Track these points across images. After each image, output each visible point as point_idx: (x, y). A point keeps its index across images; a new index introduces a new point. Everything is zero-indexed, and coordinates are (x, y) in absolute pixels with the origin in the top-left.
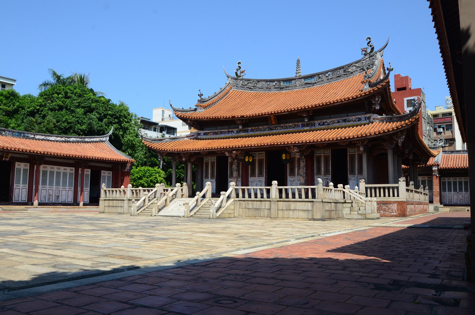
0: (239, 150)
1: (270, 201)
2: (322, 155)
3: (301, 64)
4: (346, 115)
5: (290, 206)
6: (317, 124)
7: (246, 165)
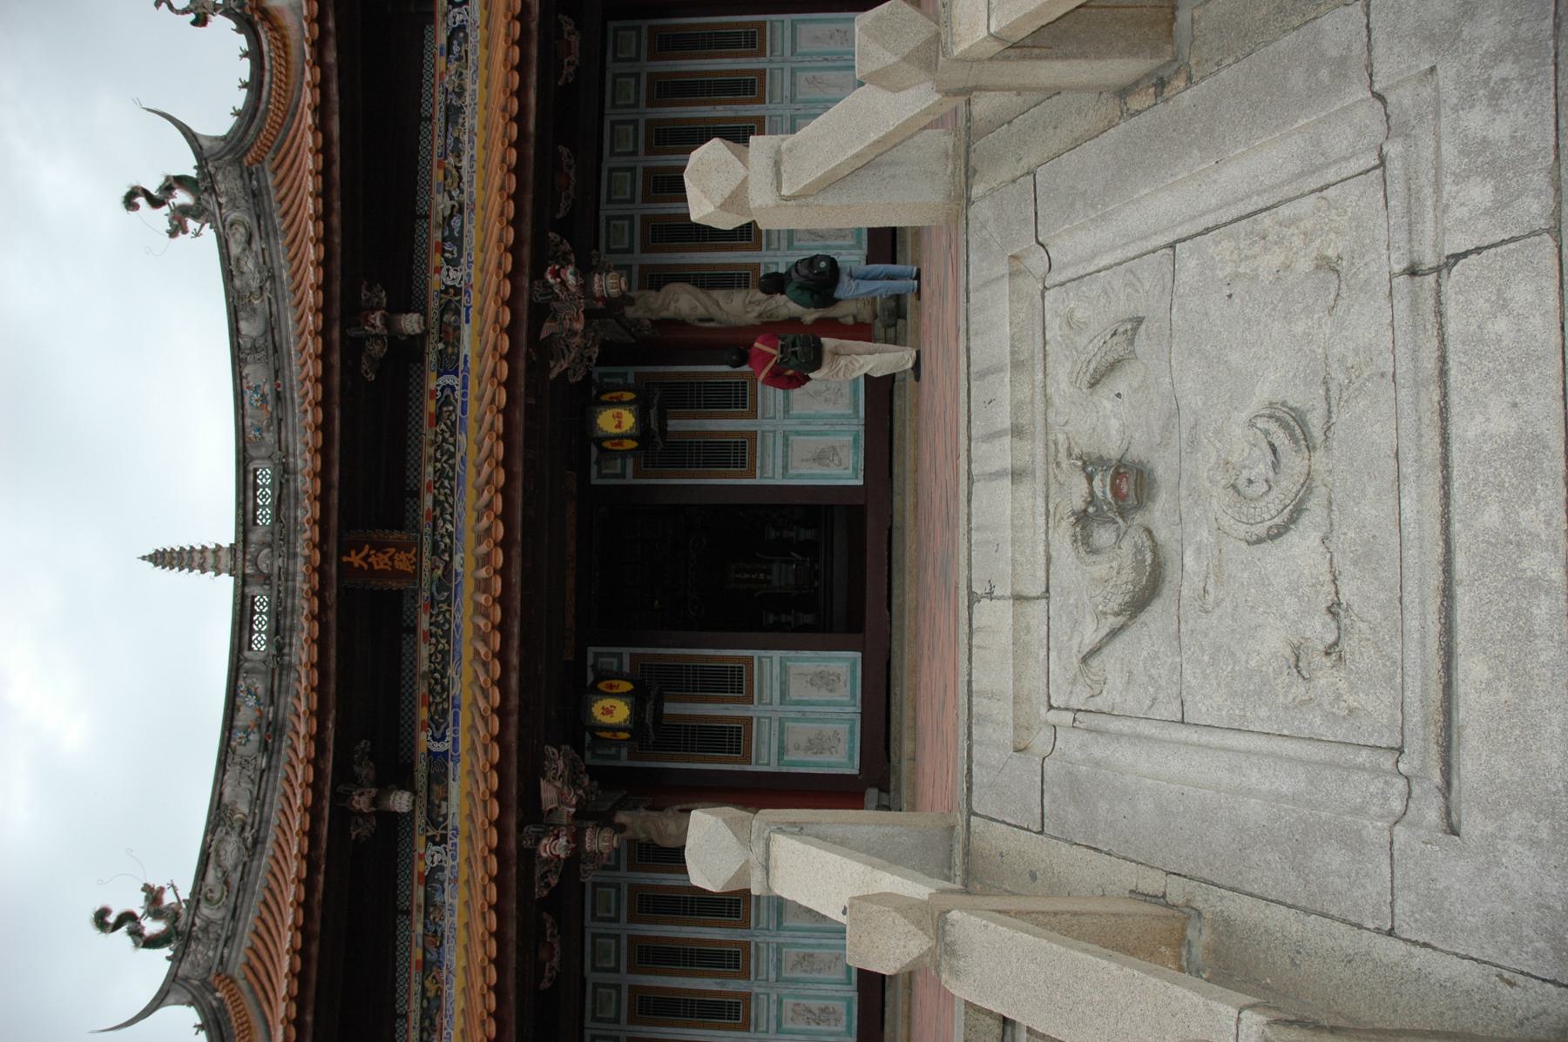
6: (453, 277)
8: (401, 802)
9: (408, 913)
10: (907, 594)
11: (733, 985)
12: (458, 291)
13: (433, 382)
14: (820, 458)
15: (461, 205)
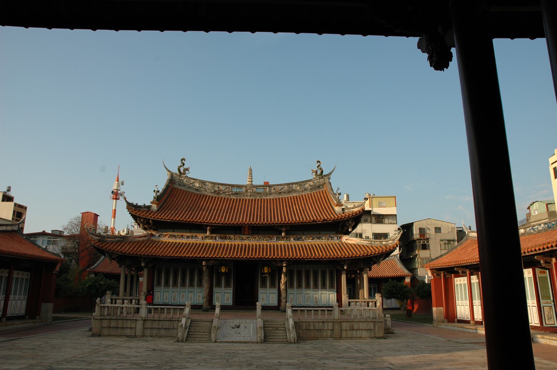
0: (214, 260)
1: (333, 322)
4: (318, 232)
5: (353, 326)
6: (292, 239)
7: (220, 274)
10: (240, 313)
11: (179, 284)
14: (263, 299)
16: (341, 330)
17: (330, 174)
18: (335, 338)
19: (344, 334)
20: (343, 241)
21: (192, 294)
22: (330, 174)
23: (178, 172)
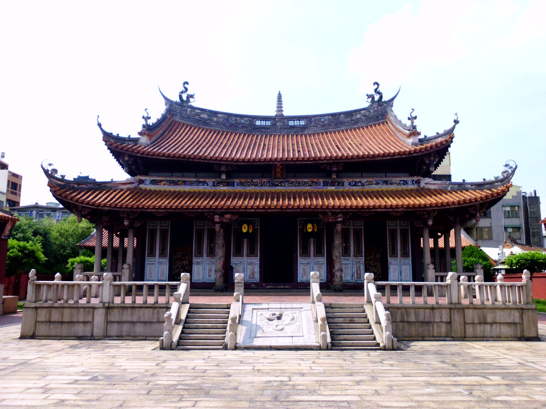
1: (450, 309)
2: (352, 228)
3: (283, 99)
4: (383, 174)
7: (240, 236)
8: (224, 177)
9: (196, 177)
12: (343, 185)
13: (321, 180)
15: (364, 185)
16: (465, 323)
17: (393, 99)
18: (454, 339)
19: (470, 330)
20: (422, 186)
21: (201, 267)
22: (393, 99)
23: (178, 100)
